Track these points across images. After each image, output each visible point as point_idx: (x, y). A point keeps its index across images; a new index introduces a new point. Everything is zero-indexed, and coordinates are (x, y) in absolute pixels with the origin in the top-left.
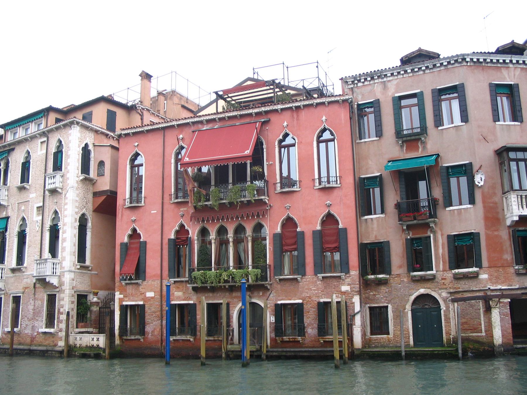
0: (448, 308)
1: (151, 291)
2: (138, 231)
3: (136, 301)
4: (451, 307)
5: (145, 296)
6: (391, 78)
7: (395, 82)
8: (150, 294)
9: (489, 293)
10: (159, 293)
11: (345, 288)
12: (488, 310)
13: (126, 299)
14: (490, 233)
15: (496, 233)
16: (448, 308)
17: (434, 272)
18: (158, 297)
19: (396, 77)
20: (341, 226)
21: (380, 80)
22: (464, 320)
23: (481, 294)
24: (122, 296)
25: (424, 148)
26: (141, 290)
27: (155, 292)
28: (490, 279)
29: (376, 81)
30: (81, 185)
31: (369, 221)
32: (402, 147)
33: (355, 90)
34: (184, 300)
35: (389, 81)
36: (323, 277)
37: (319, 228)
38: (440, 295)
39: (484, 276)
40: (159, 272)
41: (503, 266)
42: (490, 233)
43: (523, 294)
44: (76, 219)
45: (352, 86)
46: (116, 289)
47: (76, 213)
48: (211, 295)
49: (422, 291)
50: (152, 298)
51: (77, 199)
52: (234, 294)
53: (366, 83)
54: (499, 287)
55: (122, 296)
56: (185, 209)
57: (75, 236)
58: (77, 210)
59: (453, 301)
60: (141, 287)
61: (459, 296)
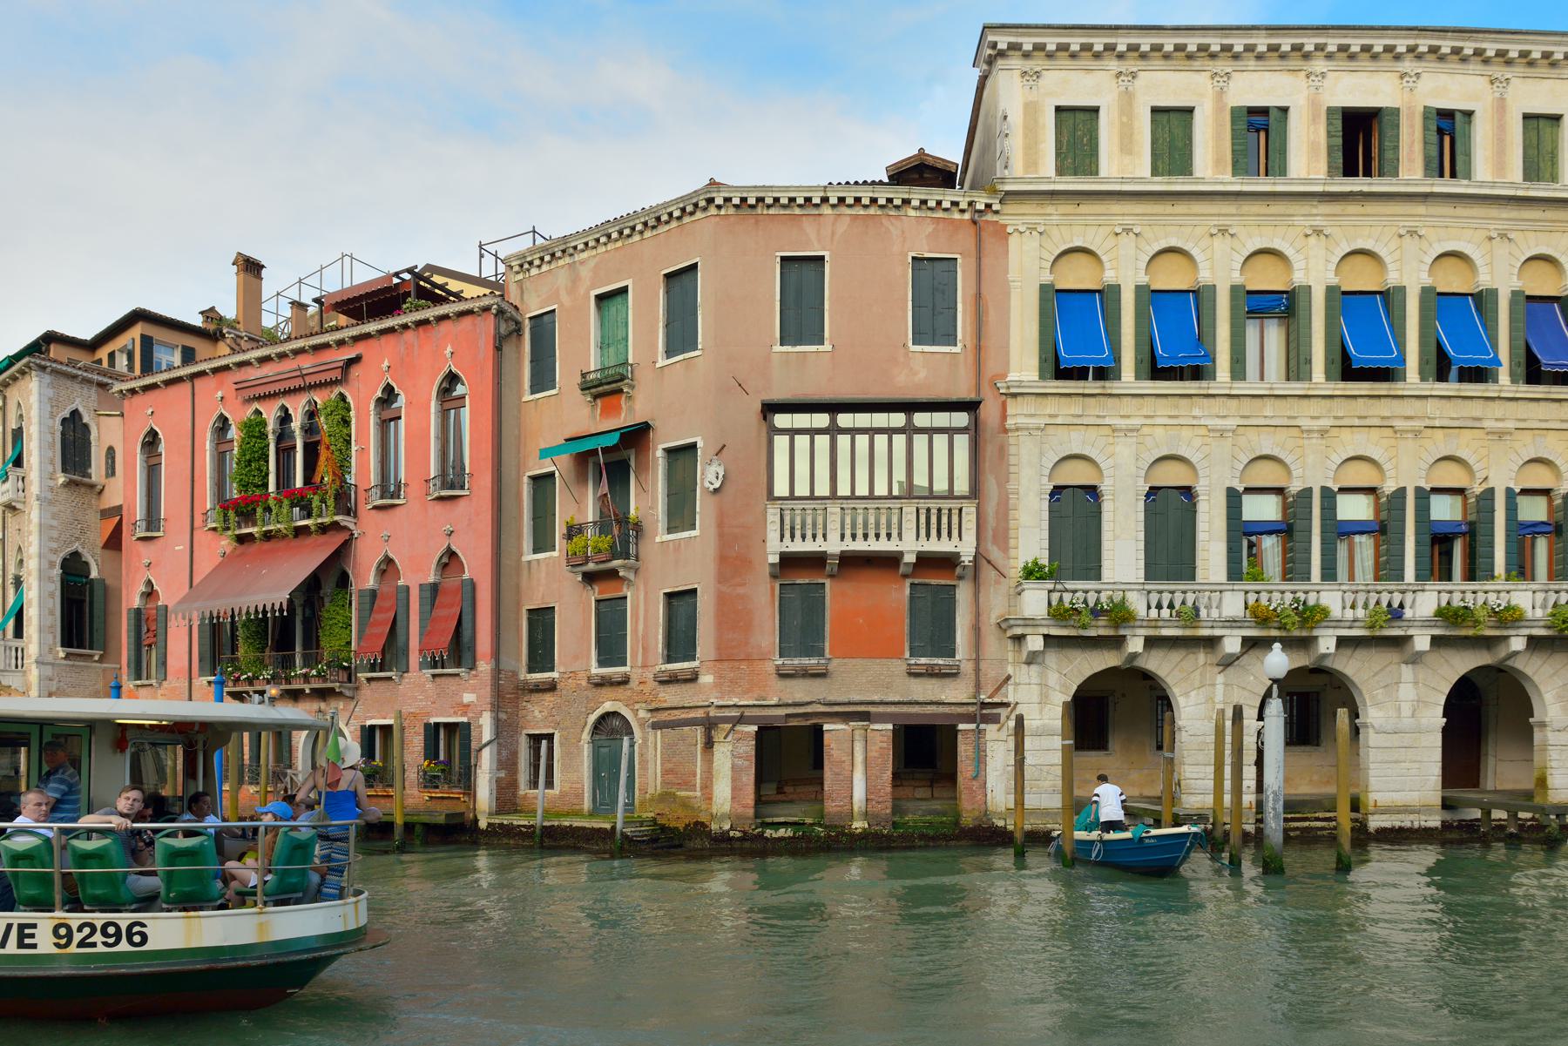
0: (645, 740)
4: (651, 738)
6: (585, 255)
7: (592, 263)
9: (713, 713)
11: (468, 698)
12: (709, 744)
14: (724, 589)
15: (741, 590)
16: (645, 740)
17: (627, 669)
19: (594, 252)
20: (466, 576)
21: (567, 260)
22: (669, 766)
23: (700, 714)
25: (631, 409)
28: (717, 685)
29: (561, 262)
30: (64, 495)
31: (534, 565)
32: (594, 407)
33: (527, 284)
35: (582, 263)
36: (434, 676)
37: (431, 579)
38: (636, 712)
39: (706, 679)
41: (748, 659)
42: (724, 589)
43: (788, 716)
44: (52, 565)
45: (520, 277)
47: (55, 552)
49: (608, 706)
51: (55, 523)
54: (735, 701)
57: (52, 595)
58: (54, 545)
59: (656, 726)
61: (664, 716)
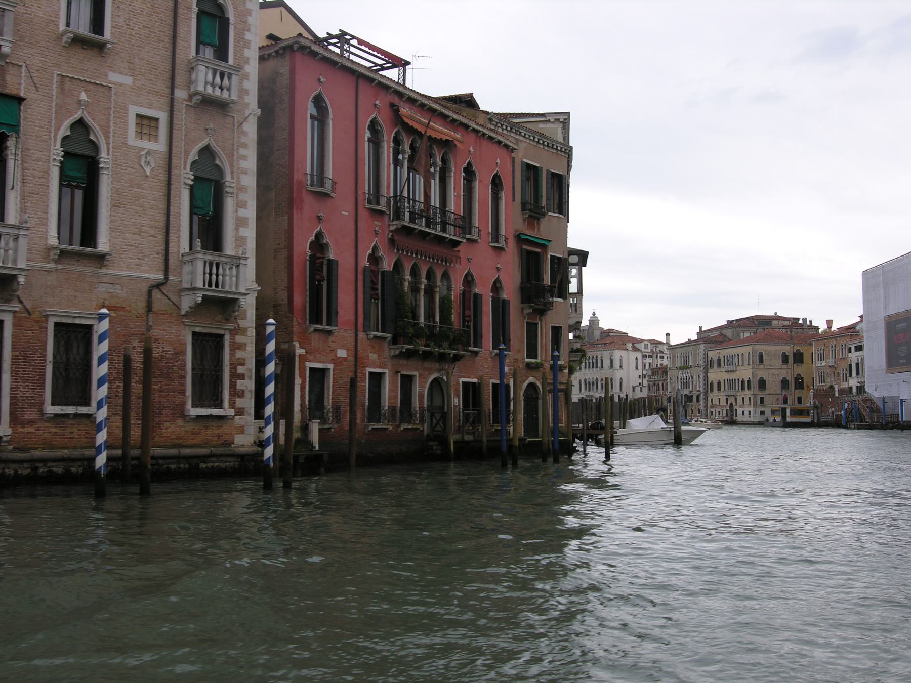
1: (343, 347)
2: (327, 239)
3: (324, 363)
5: (336, 355)
8: (342, 353)
10: (353, 353)
13: (311, 358)
17: (539, 360)
18: (351, 358)
24: (303, 351)
26: (331, 344)
27: (348, 350)
34: (380, 367)
40: (352, 318)
46: (295, 338)
48: (405, 362)
50: (345, 359)
52: (427, 364)
53: (505, 132)
55: (303, 351)
56: (379, 223)
60: (331, 338)
